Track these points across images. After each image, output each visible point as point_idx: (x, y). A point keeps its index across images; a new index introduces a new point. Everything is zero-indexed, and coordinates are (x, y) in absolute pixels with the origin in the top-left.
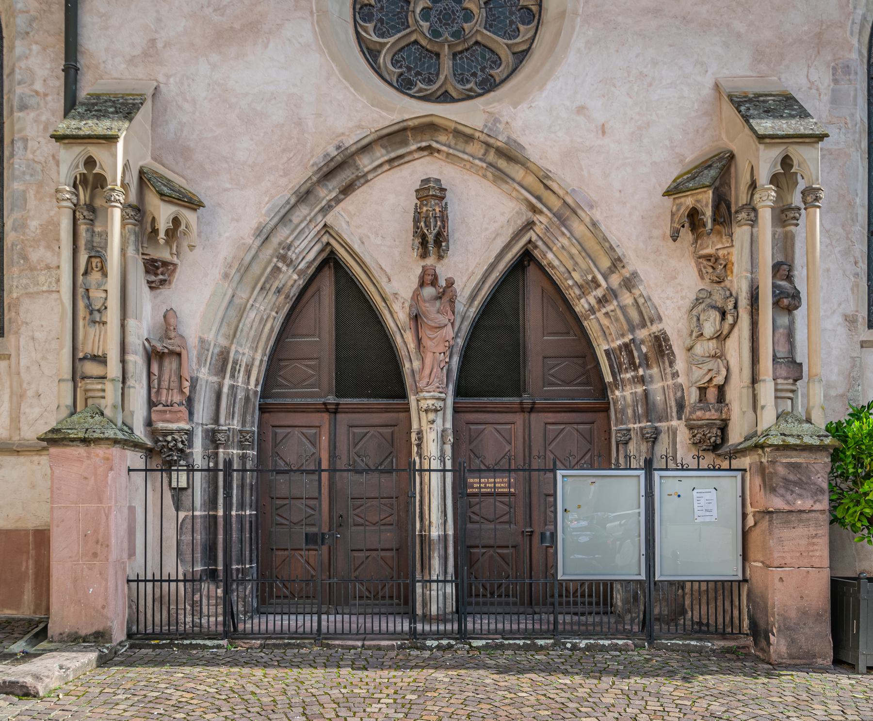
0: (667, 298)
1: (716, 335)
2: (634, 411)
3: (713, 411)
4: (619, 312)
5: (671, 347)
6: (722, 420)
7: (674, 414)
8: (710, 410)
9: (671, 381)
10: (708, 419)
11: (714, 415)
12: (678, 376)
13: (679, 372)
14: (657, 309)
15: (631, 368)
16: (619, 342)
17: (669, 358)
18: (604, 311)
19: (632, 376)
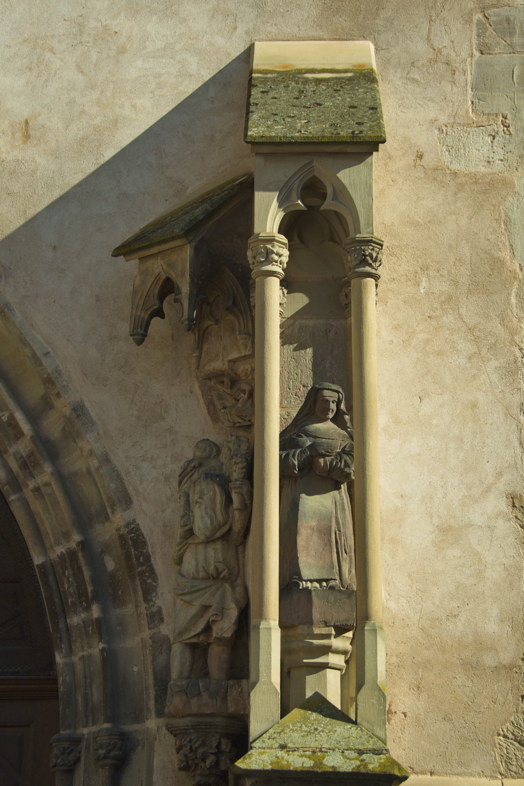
0: (144, 459)
1: (218, 534)
2: (86, 698)
3: (205, 696)
4: (56, 488)
5: (148, 558)
6: (231, 717)
7: (152, 704)
8: (199, 694)
9: (148, 631)
10: (196, 715)
12: (162, 620)
13: (164, 612)
14: (121, 480)
15: (81, 603)
16: (60, 550)
17: (143, 583)
18: (32, 484)
19: (83, 621)
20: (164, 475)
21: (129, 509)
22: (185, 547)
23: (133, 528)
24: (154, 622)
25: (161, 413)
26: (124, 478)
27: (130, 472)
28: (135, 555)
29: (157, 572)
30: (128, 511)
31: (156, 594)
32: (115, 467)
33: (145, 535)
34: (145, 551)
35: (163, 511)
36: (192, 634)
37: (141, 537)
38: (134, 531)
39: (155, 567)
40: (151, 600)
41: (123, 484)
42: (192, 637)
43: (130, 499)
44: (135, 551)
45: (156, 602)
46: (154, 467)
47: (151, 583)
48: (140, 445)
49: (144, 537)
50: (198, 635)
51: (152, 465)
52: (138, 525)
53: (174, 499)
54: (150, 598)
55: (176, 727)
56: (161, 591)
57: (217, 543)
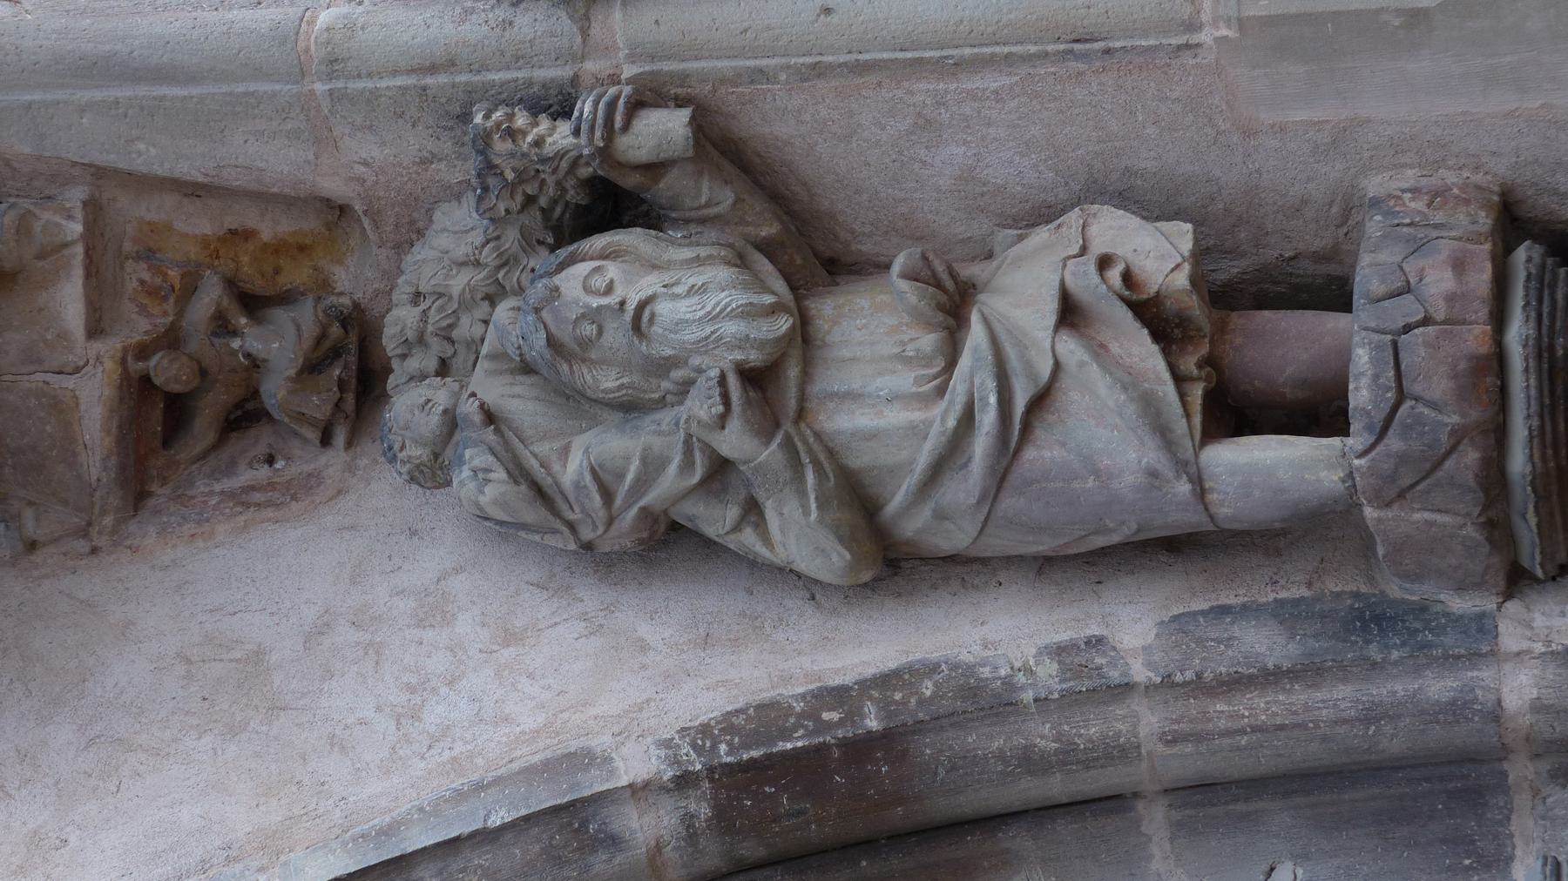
1: (780, 285)
11: (1459, 266)
12: (1096, 643)
13: (1063, 636)
14: (480, 787)
20: (495, 647)
21: (608, 760)
22: (811, 440)
23: (694, 746)
24: (1099, 668)
25: (237, 661)
26: (475, 777)
27: (454, 759)
28: (809, 734)
29: (893, 665)
30: (619, 764)
31: (984, 665)
32: (421, 809)
33: (729, 708)
34: (799, 707)
35: (643, 647)
36: (1169, 390)
37: (739, 720)
38: (708, 744)
39: (870, 671)
40: (1008, 683)
41: (497, 781)
42: (1182, 396)
43: (569, 756)
44: (789, 738)
45: (1017, 665)
46: (451, 683)
47: (936, 684)
48: (346, 727)
49: (738, 712)
50: (1179, 379)
51: (444, 690)
52: (684, 729)
53: (603, 614)
54: (999, 683)
55: (1541, 416)
56: (976, 648)
57: (813, 312)
